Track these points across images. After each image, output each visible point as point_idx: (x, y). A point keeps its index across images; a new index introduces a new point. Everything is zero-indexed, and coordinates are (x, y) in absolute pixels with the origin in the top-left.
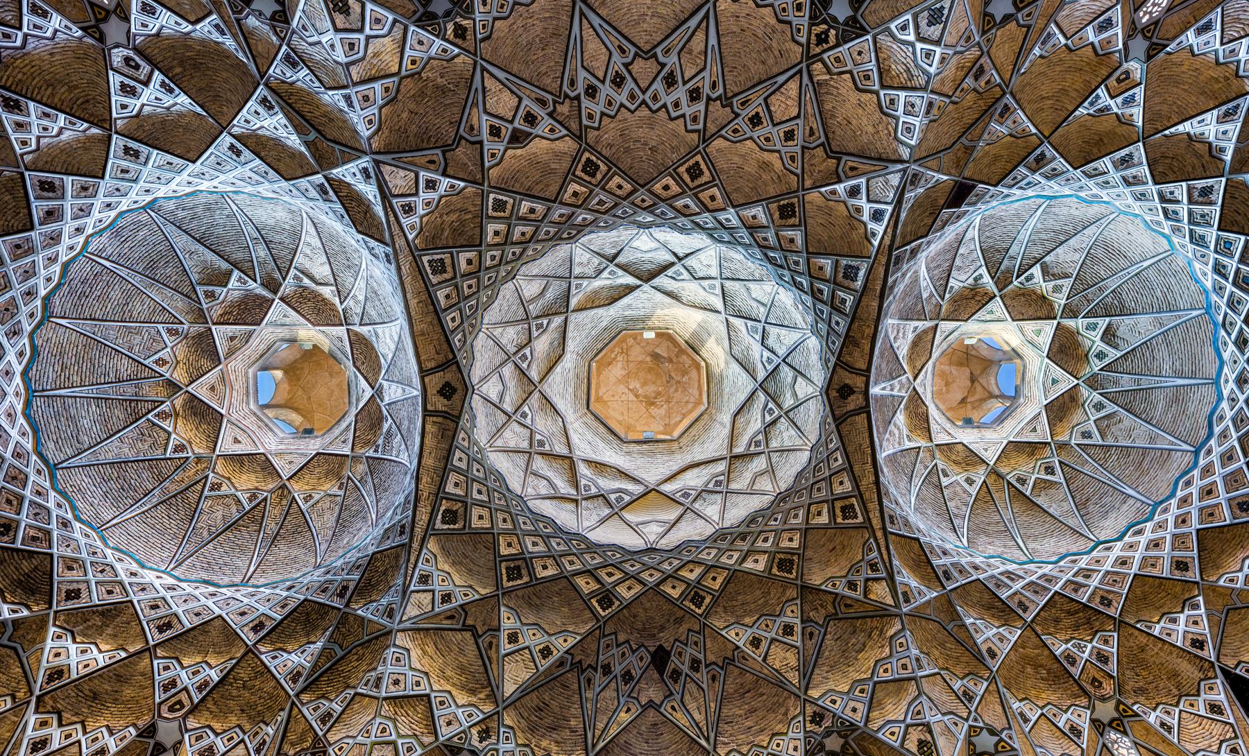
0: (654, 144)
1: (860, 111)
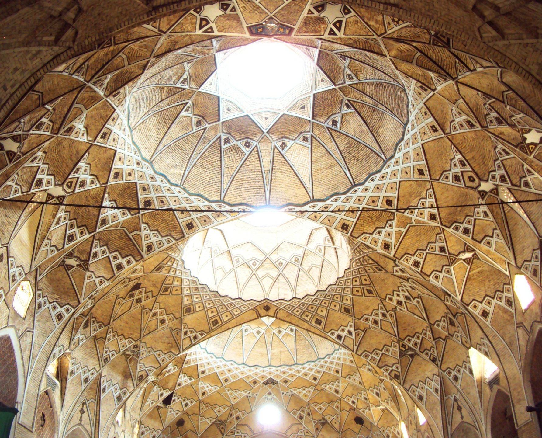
0: (386, 281)
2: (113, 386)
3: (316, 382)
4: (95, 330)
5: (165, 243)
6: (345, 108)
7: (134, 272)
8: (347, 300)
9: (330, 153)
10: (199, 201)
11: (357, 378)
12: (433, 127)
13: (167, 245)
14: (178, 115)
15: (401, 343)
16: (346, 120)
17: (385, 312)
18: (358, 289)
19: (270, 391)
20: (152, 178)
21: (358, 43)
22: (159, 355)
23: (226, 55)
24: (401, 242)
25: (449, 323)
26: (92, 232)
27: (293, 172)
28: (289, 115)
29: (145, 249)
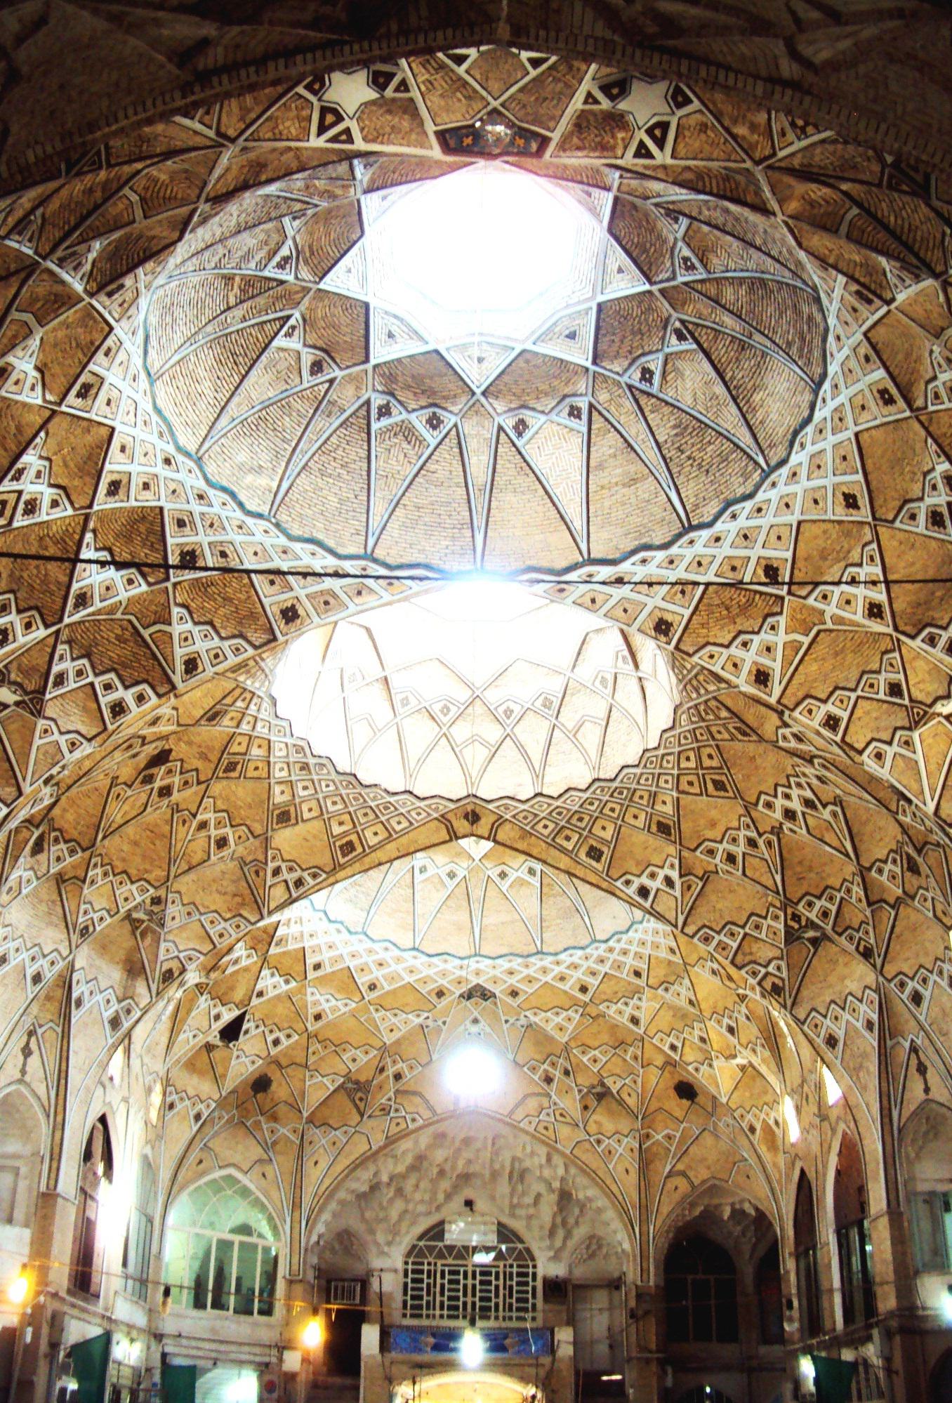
0: (759, 761)
1: (737, 905)
2: (101, 992)
3: (586, 998)
4: (58, 859)
5: (229, 653)
6: (674, 340)
7: (154, 722)
8: (664, 803)
9: (632, 448)
10: (313, 554)
11: (683, 991)
12: (883, 393)
13: (232, 660)
14: (267, 346)
15: (789, 911)
16: (676, 370)
17: (754, 835)
18: (691, 778)
19: (476, 1014)
20: (201, 497)
21: (707, 179)
22: (212, 922)
23: (386, 203)
24: (796, 669)
25: (905, 866)
26: (54, 624)
27: (541, 491)
28: (536, 354)
29: (180, 667)
